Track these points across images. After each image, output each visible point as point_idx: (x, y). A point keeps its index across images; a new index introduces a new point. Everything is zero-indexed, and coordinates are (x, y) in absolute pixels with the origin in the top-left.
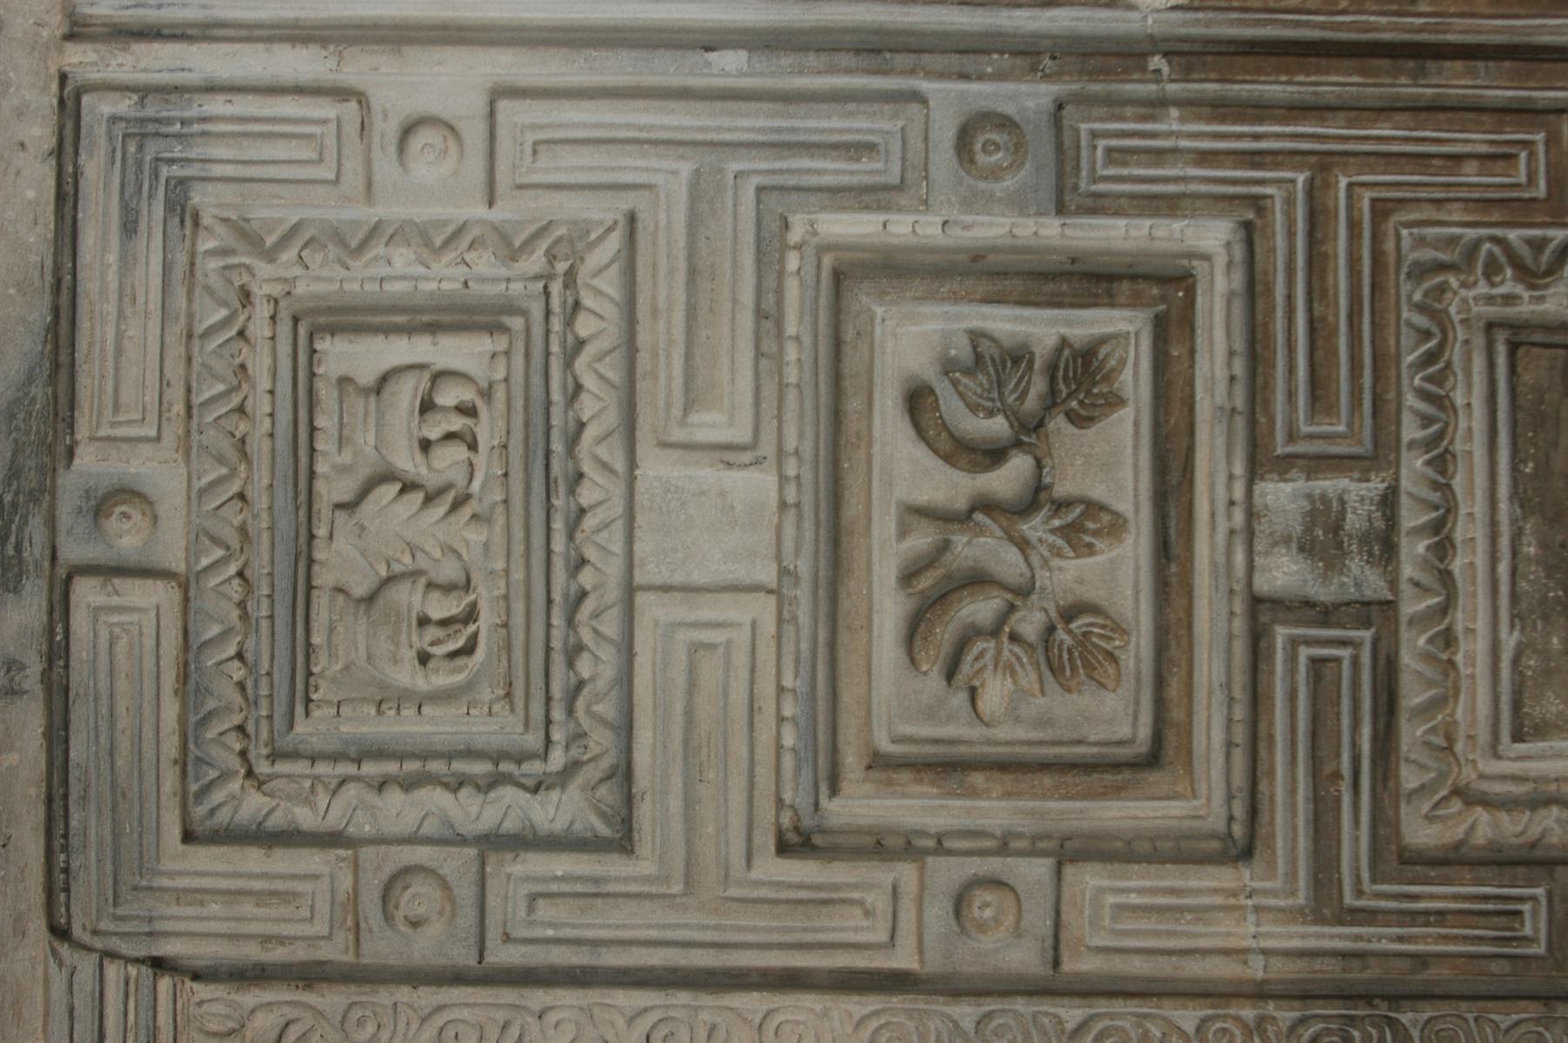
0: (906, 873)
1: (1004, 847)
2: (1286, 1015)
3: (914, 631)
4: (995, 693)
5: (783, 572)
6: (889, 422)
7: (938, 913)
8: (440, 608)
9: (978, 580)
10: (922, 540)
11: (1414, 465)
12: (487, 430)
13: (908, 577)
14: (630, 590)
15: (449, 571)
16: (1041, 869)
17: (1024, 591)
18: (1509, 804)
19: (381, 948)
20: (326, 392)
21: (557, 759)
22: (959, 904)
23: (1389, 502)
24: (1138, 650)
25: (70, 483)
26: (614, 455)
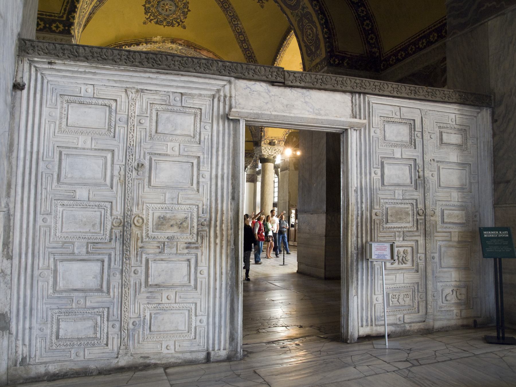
0: (419, 264)
1: (417, 257)
2: (427, 238)
3: (405, 264)
4: (409, 258)
5: (402, 273)
6: (393, 266)
7: (421, 261)
8: (405, 296)
9: (402, 260)
10: (400, 263)
11: (395, 230)
12: (395, 294)
13: (402, 264)
14: (404, 283)
15: (403, 296)
16: (418, 254)
17: (403, 256)
18: (414, 223)
19: (424, 299)
20: (393, 305)
21: (413, 288)
22: (421, 260)
23: (398, 231)
24: (406, 248)
25: (399, 323)
26: (395, 285)
